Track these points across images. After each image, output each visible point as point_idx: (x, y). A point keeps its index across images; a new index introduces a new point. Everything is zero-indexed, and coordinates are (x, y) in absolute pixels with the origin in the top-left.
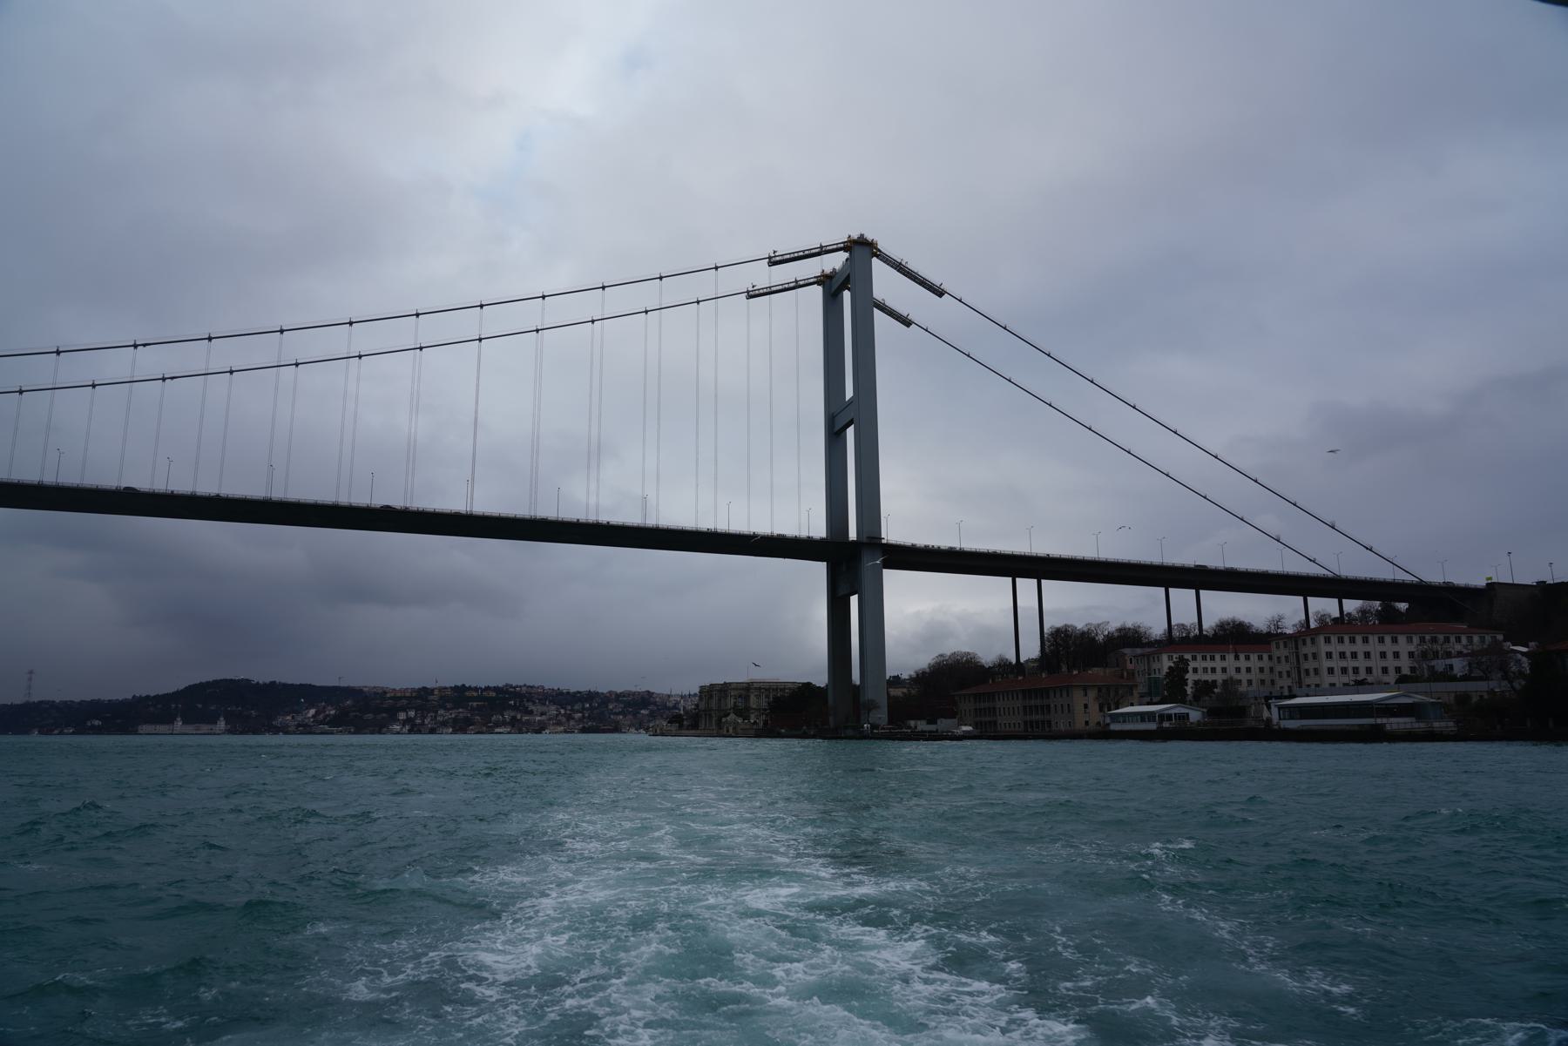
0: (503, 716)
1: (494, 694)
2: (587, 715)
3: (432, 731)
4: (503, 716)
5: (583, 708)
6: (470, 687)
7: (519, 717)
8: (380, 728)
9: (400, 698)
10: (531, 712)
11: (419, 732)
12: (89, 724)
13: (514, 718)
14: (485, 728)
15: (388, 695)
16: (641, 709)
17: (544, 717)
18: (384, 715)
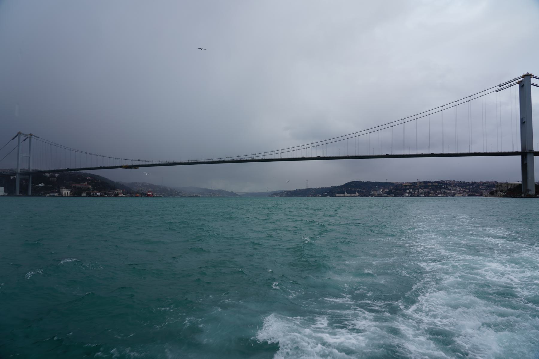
0: (440, 191)
1: (437, 184)
2: (471, 190)
3: (418, 196)
4: (440, 191)
5: (470, 188)
6: (429, 182)
7: (446, 191)
8: (402, 195)
9: (407, 186)
10: (450, 190)
11: (414, 196)
12: (324, 194)
13: (444, 192)
14: (435, 195)
15: (403, 185)
16: (493, 188)
17: (455, 191)
18: (403, 191)
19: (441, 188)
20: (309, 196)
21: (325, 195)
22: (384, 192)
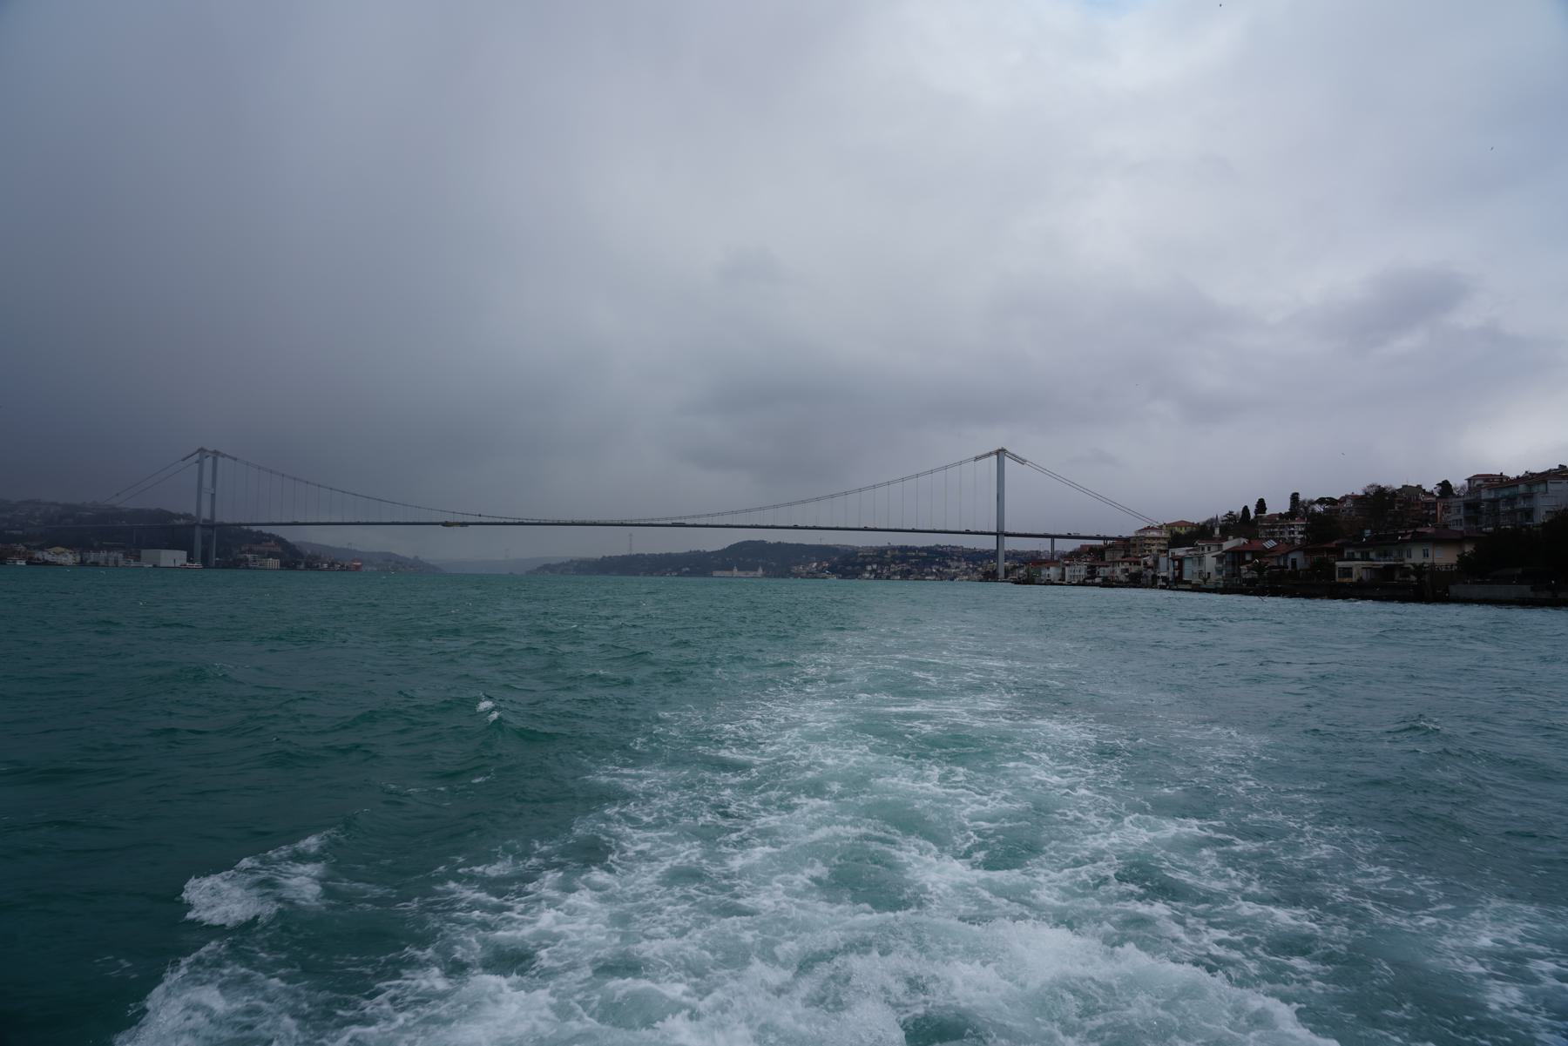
1: (925, 554)
3: (888, 578)
6: (911, 547)
7: (941, 569)
8: (855, 575)
10: (949, 567)
15: (860, 554)
17: (957, 570)
18: (858, 567)
19: (932, 563)
20: (638, 575)
21: (687, 572)
22: (820, 568)
